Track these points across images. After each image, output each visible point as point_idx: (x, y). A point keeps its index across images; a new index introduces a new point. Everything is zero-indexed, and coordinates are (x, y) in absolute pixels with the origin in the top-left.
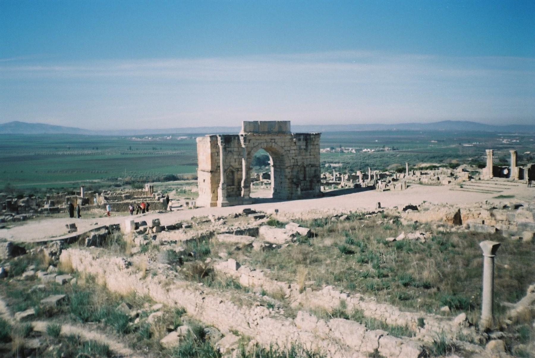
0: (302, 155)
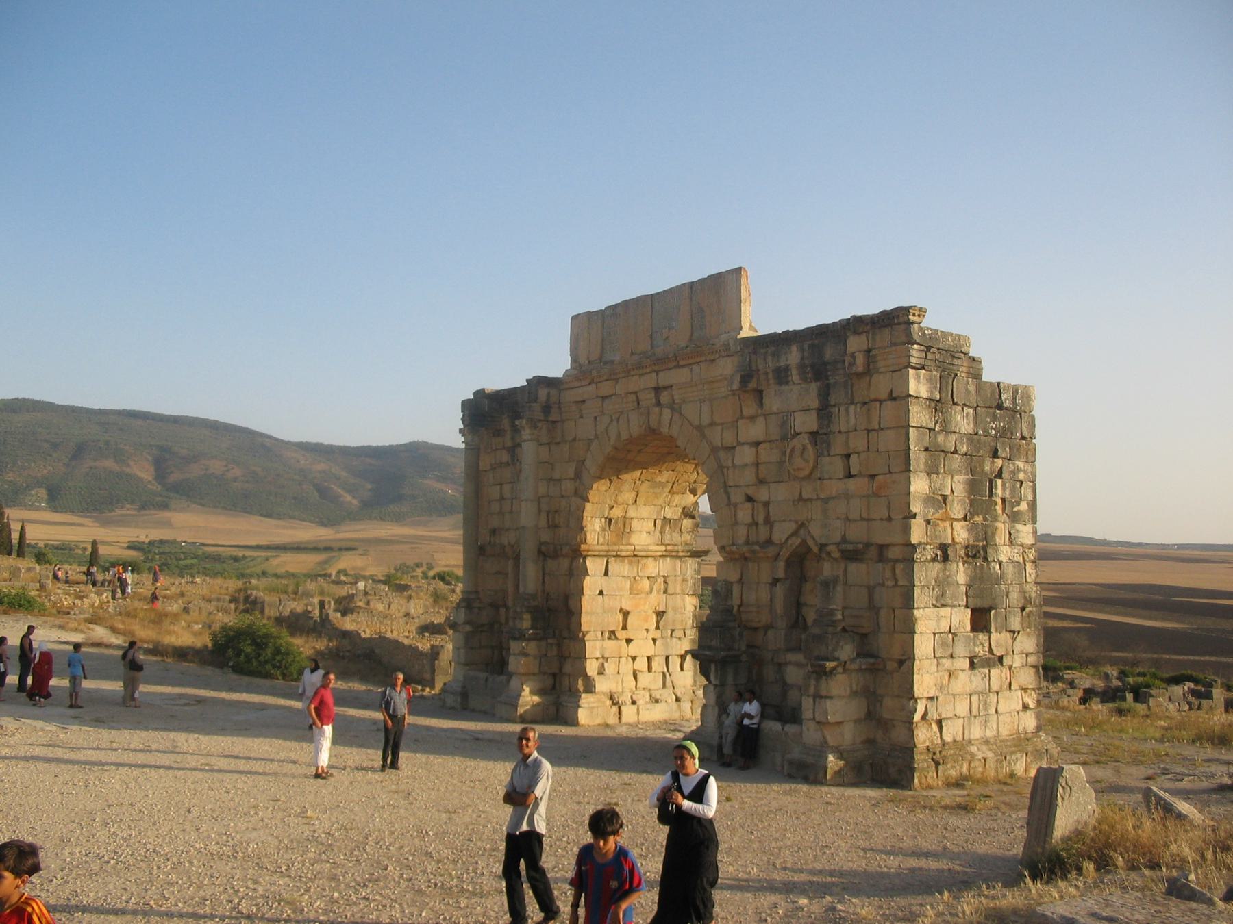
0: (796, 478)
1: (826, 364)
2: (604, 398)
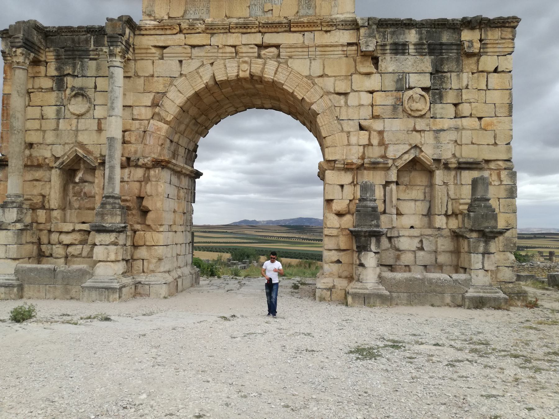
0: (409, 116)
1: (442, 44)
2: (193, 47)
